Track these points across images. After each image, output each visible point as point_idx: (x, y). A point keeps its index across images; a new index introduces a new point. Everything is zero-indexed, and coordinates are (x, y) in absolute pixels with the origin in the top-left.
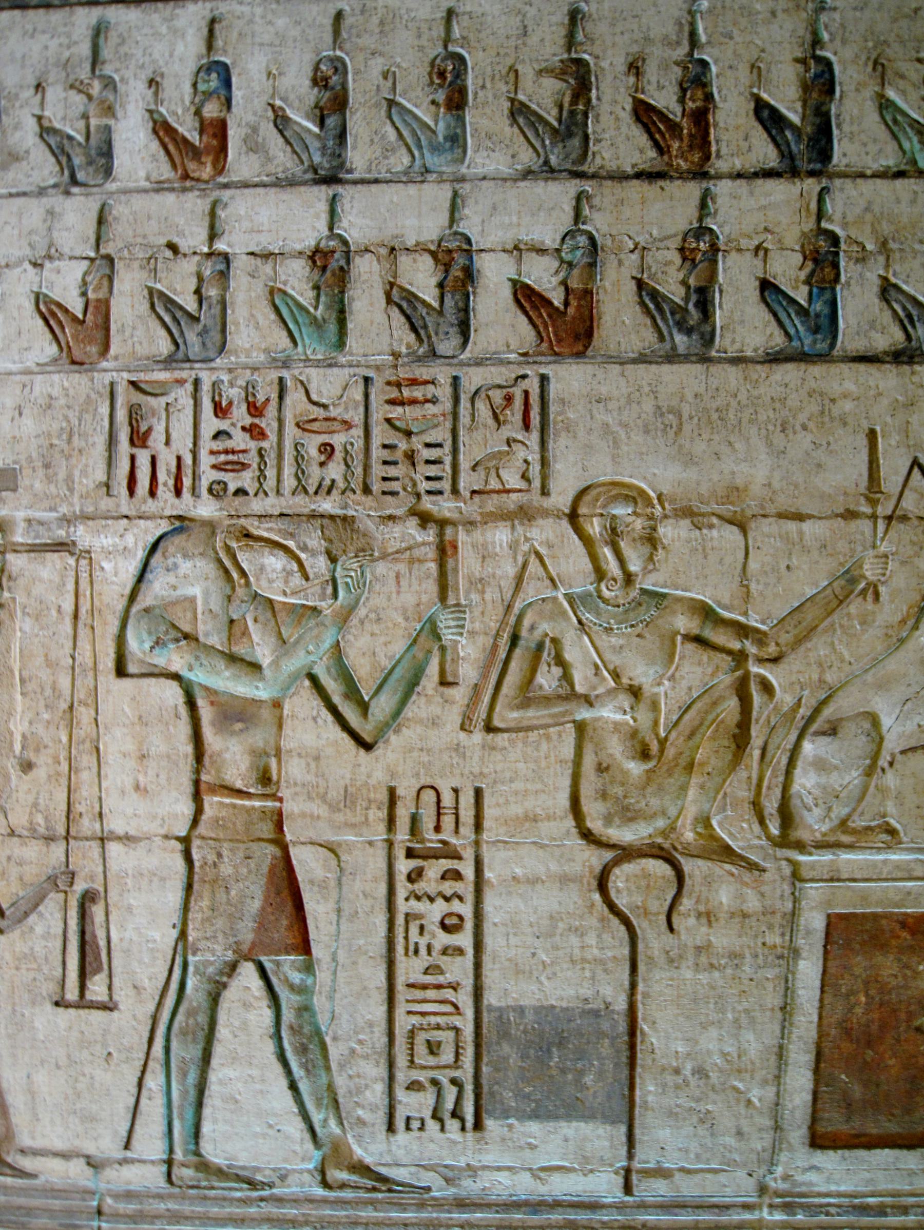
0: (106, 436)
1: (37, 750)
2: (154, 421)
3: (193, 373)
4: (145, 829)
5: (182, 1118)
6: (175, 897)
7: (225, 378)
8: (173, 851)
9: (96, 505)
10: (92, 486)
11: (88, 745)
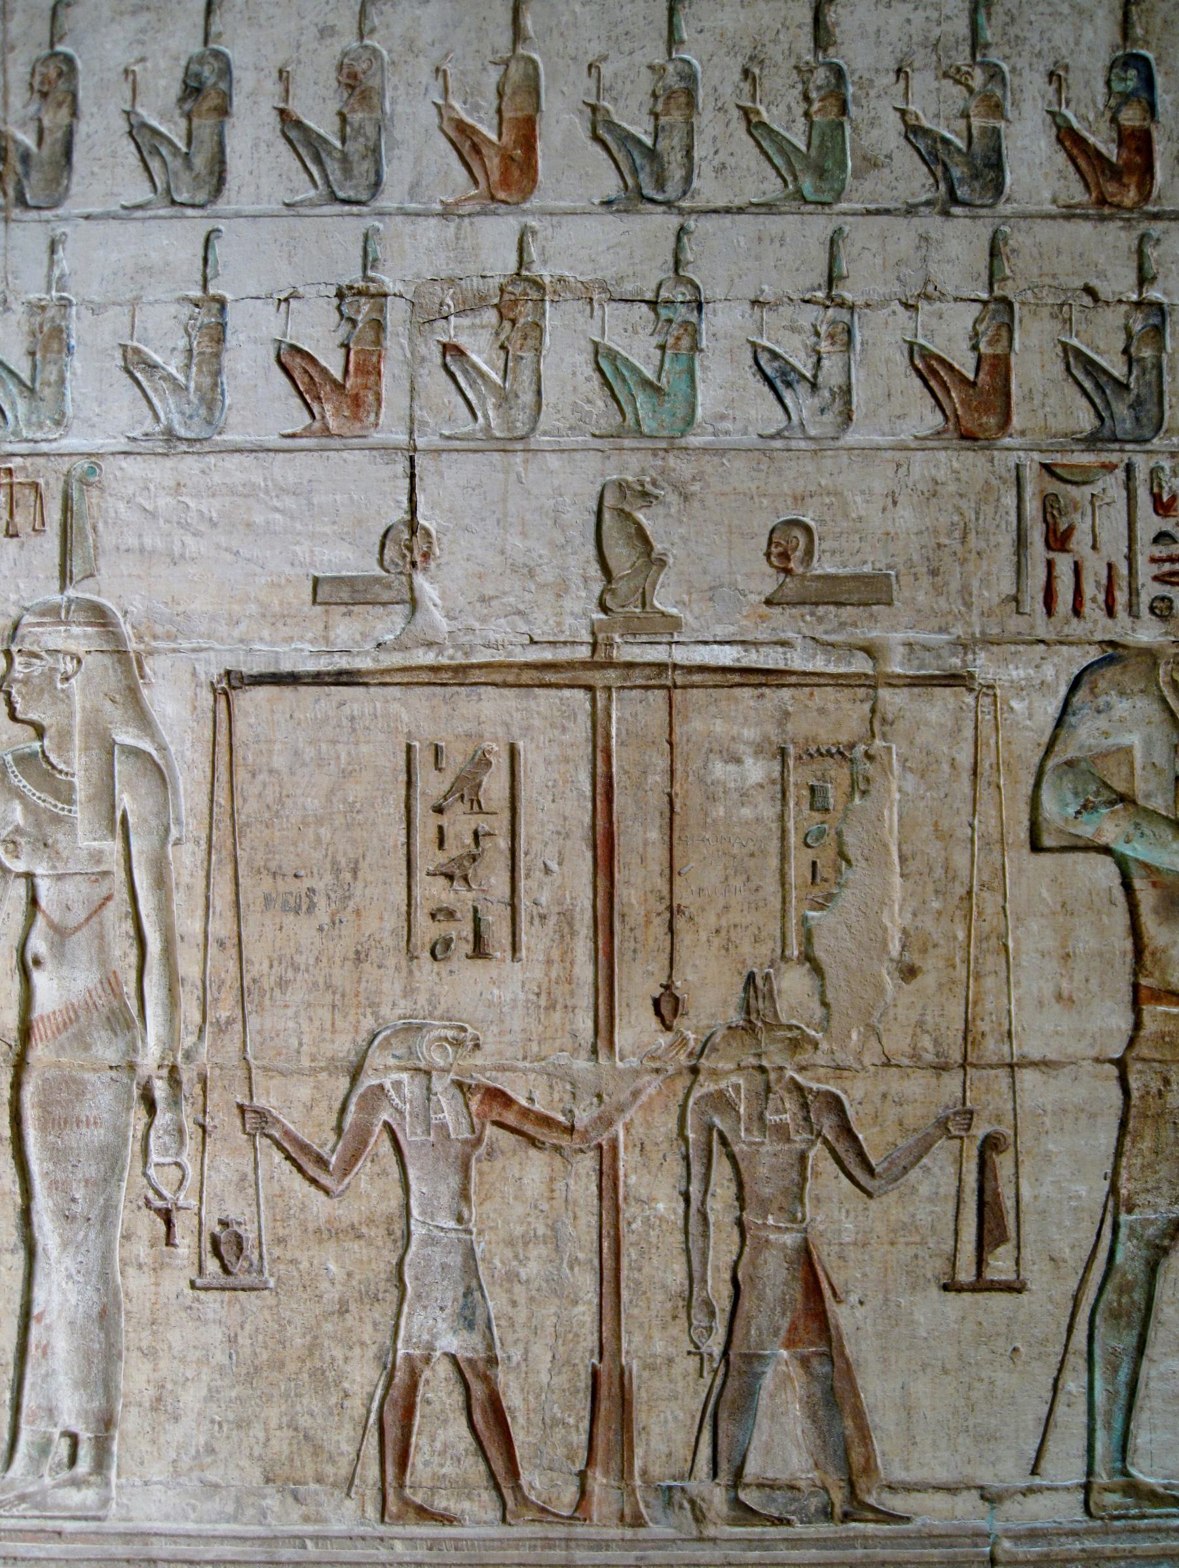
0: (1014, 535)
1: (924, 951)
2: (1076, 517)
3: (1125, 457)
4: (1070, 1051)
5: (1108, 1426)
6: (1107, 1138)
7: (1167, 464)
8: (1107, 1078)
9: (1001, 624)
10: (996, 600)
11: (993, 942)
